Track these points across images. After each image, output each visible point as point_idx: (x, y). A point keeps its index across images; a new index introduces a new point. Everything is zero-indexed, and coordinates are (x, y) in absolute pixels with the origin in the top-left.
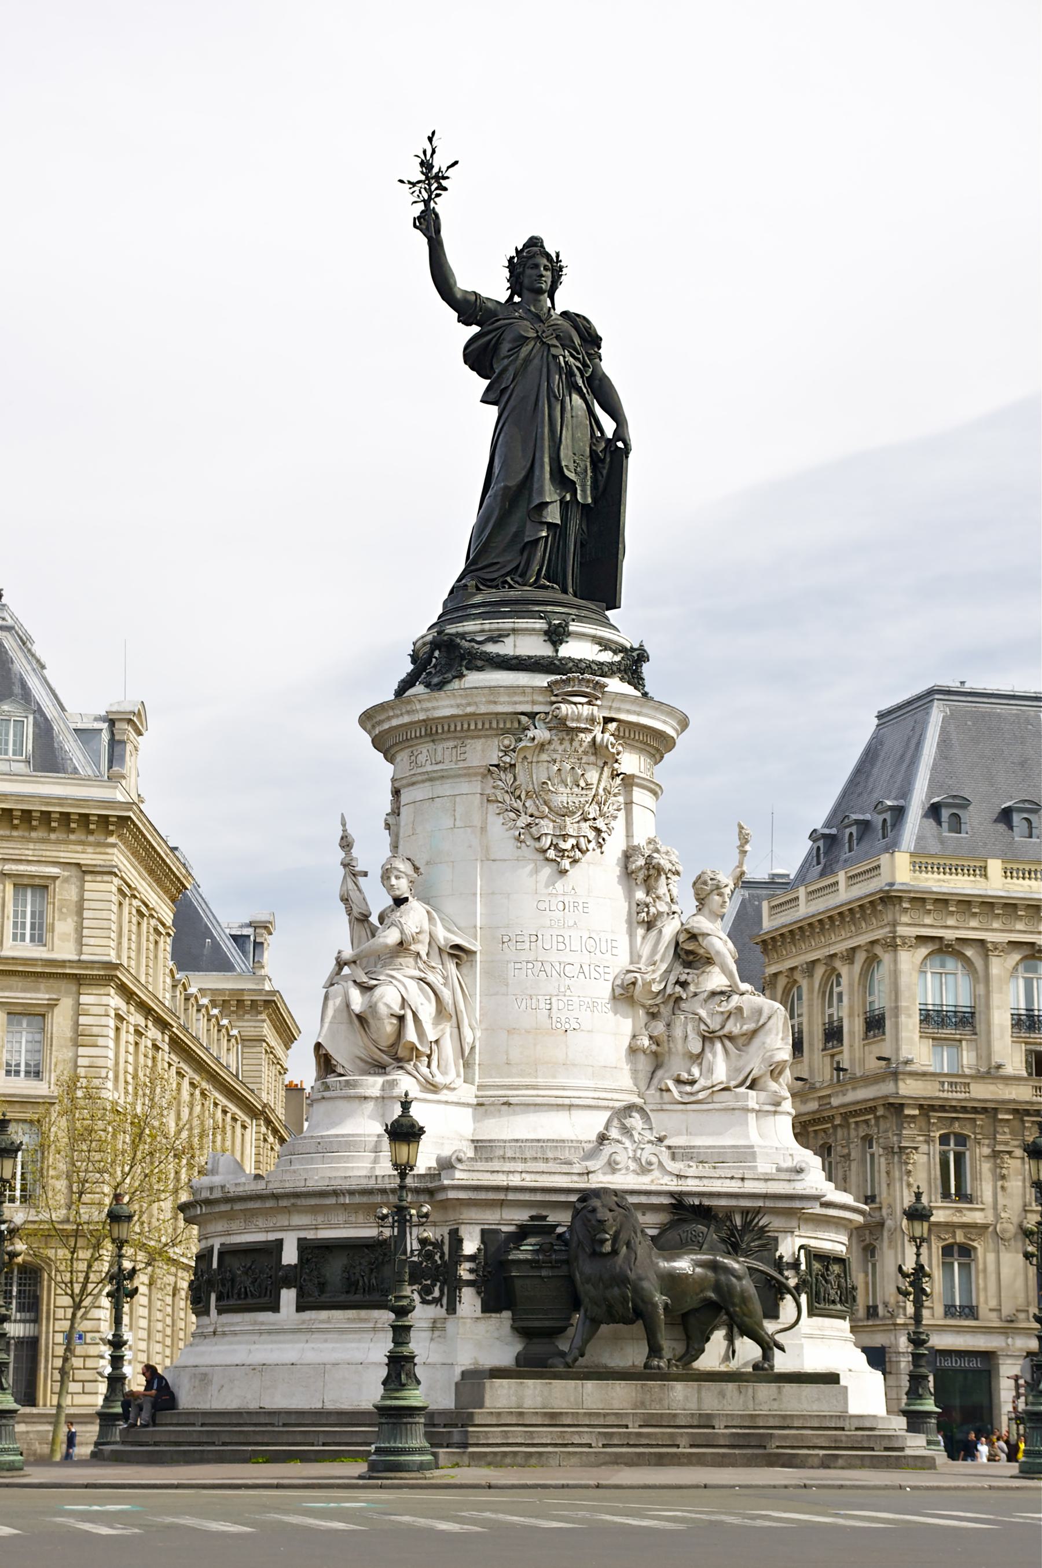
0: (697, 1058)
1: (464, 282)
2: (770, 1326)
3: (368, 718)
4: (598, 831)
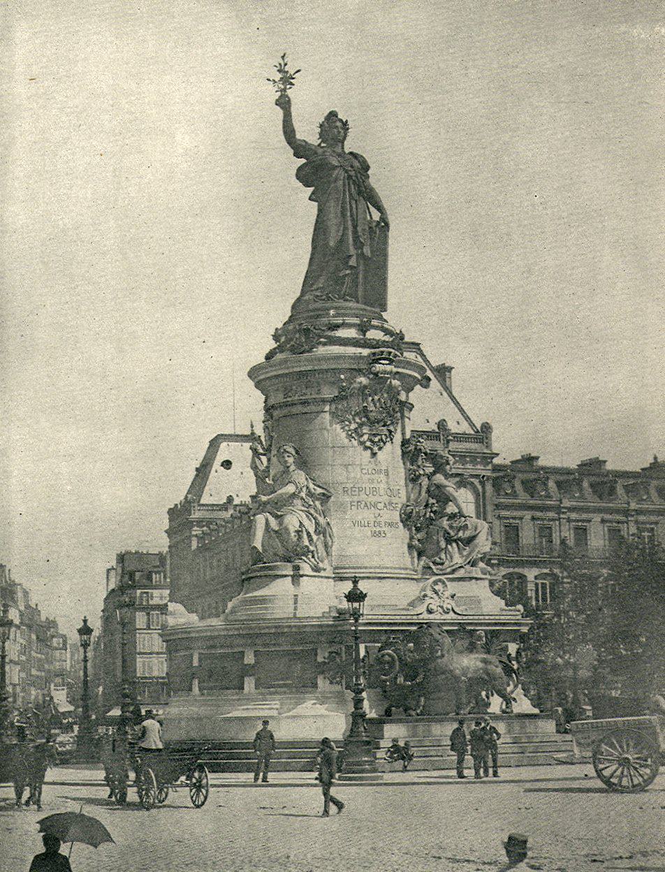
1: (299, 136)
3: (253, 373)
4: (390, 432)
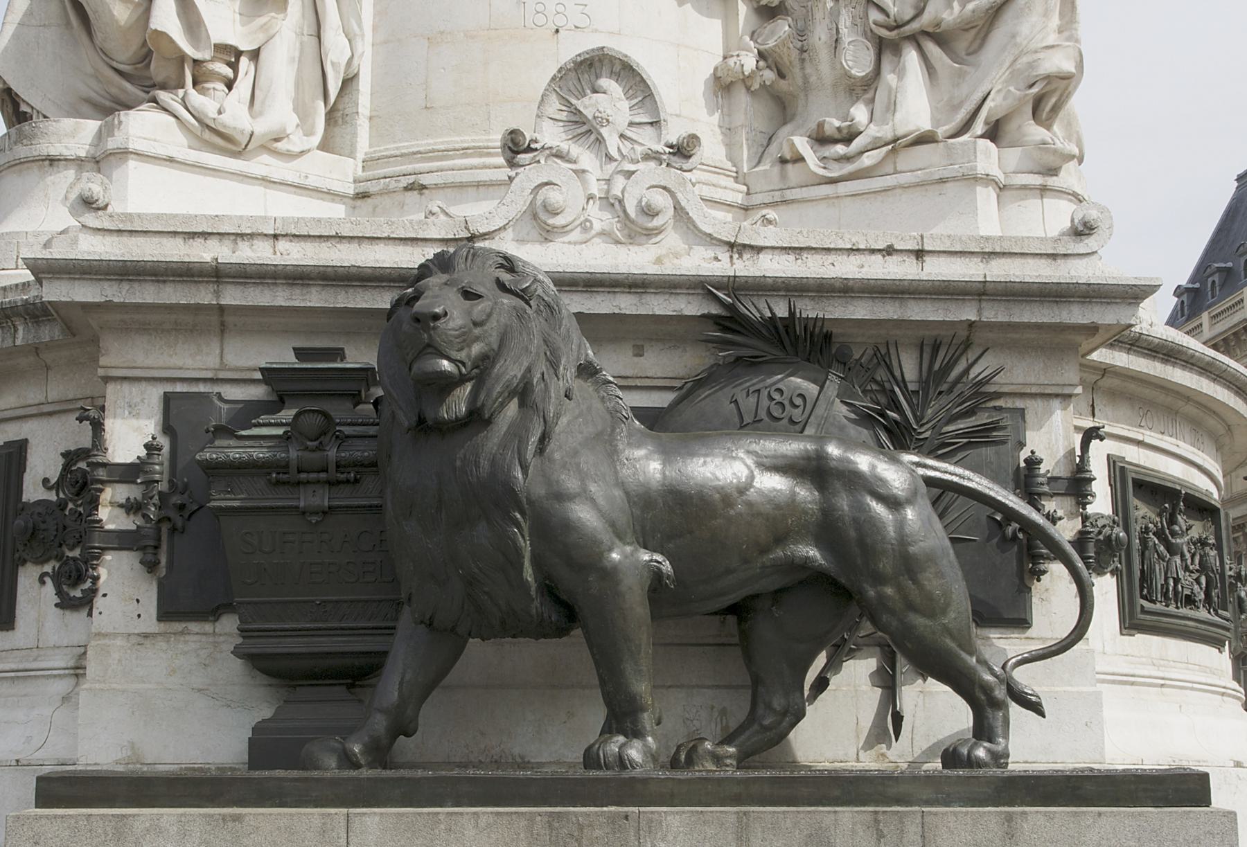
0: (865, 88)
2: (1004, 646)
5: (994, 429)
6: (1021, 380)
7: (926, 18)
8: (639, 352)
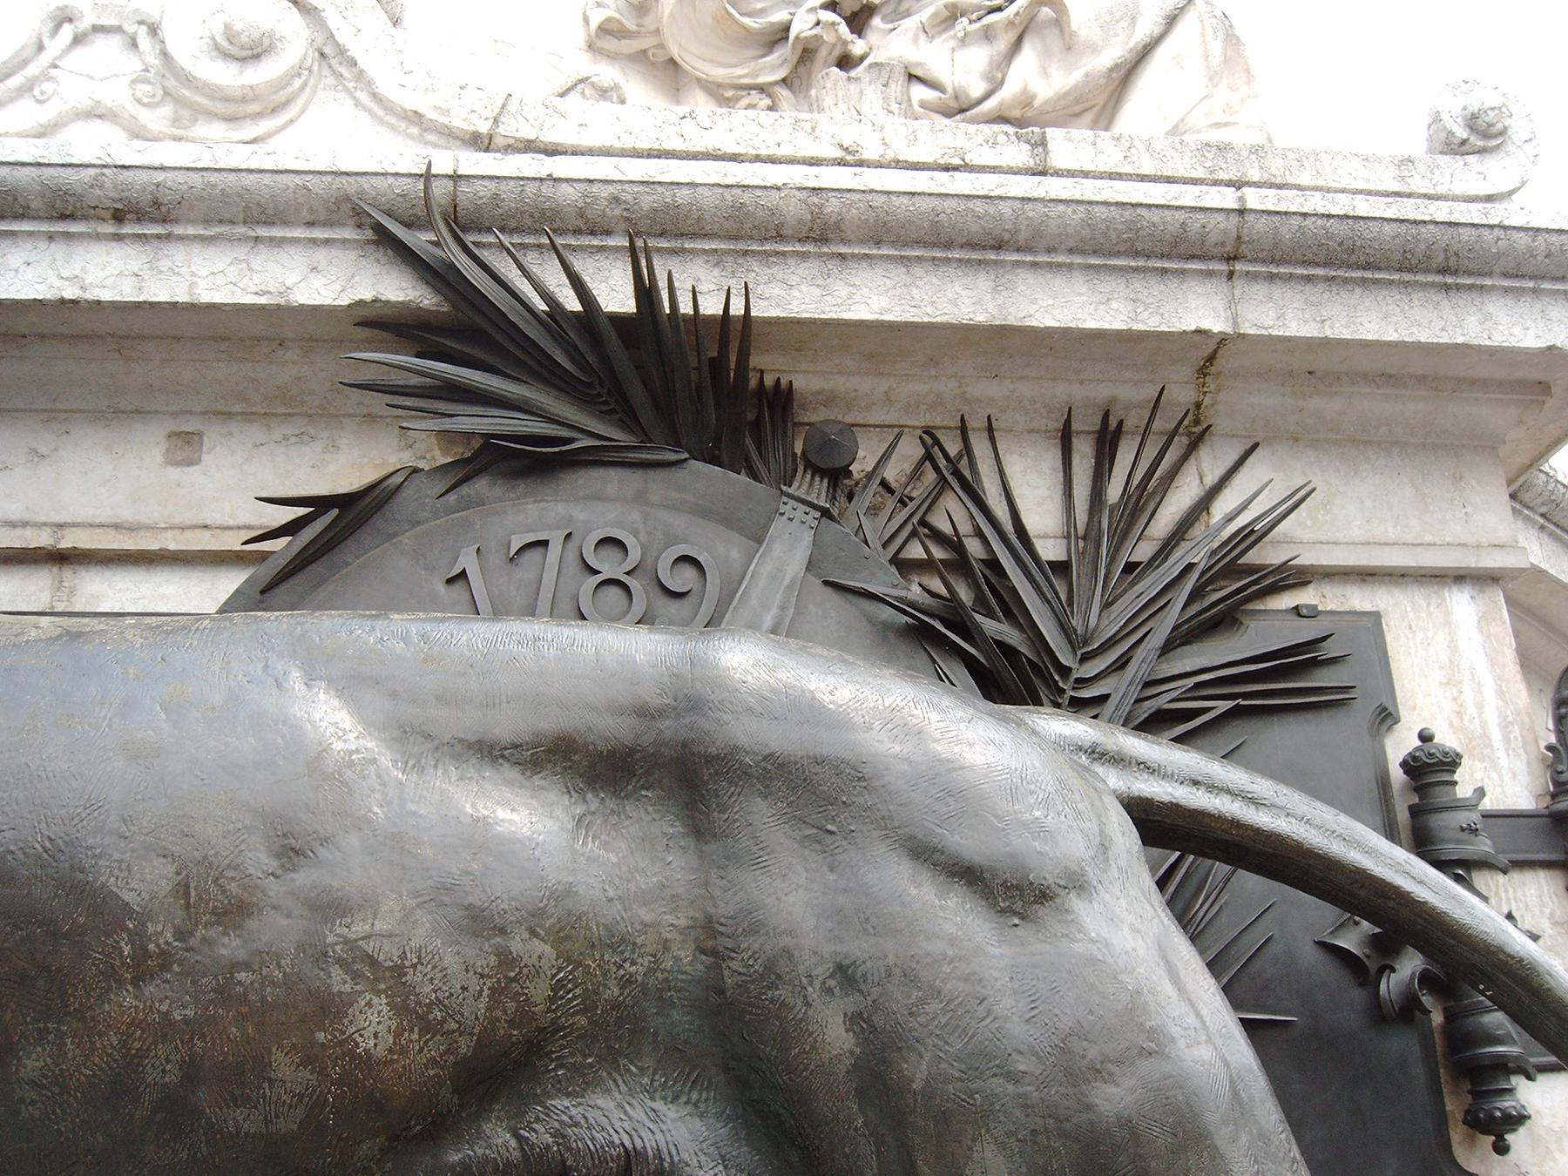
5: (1315, 663)
6: (1357, 533)
7: (1008, 92)
8: (185, 447)
